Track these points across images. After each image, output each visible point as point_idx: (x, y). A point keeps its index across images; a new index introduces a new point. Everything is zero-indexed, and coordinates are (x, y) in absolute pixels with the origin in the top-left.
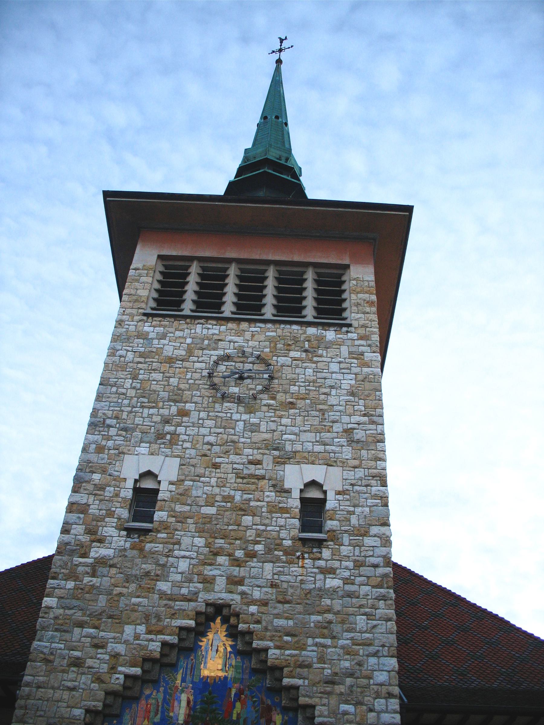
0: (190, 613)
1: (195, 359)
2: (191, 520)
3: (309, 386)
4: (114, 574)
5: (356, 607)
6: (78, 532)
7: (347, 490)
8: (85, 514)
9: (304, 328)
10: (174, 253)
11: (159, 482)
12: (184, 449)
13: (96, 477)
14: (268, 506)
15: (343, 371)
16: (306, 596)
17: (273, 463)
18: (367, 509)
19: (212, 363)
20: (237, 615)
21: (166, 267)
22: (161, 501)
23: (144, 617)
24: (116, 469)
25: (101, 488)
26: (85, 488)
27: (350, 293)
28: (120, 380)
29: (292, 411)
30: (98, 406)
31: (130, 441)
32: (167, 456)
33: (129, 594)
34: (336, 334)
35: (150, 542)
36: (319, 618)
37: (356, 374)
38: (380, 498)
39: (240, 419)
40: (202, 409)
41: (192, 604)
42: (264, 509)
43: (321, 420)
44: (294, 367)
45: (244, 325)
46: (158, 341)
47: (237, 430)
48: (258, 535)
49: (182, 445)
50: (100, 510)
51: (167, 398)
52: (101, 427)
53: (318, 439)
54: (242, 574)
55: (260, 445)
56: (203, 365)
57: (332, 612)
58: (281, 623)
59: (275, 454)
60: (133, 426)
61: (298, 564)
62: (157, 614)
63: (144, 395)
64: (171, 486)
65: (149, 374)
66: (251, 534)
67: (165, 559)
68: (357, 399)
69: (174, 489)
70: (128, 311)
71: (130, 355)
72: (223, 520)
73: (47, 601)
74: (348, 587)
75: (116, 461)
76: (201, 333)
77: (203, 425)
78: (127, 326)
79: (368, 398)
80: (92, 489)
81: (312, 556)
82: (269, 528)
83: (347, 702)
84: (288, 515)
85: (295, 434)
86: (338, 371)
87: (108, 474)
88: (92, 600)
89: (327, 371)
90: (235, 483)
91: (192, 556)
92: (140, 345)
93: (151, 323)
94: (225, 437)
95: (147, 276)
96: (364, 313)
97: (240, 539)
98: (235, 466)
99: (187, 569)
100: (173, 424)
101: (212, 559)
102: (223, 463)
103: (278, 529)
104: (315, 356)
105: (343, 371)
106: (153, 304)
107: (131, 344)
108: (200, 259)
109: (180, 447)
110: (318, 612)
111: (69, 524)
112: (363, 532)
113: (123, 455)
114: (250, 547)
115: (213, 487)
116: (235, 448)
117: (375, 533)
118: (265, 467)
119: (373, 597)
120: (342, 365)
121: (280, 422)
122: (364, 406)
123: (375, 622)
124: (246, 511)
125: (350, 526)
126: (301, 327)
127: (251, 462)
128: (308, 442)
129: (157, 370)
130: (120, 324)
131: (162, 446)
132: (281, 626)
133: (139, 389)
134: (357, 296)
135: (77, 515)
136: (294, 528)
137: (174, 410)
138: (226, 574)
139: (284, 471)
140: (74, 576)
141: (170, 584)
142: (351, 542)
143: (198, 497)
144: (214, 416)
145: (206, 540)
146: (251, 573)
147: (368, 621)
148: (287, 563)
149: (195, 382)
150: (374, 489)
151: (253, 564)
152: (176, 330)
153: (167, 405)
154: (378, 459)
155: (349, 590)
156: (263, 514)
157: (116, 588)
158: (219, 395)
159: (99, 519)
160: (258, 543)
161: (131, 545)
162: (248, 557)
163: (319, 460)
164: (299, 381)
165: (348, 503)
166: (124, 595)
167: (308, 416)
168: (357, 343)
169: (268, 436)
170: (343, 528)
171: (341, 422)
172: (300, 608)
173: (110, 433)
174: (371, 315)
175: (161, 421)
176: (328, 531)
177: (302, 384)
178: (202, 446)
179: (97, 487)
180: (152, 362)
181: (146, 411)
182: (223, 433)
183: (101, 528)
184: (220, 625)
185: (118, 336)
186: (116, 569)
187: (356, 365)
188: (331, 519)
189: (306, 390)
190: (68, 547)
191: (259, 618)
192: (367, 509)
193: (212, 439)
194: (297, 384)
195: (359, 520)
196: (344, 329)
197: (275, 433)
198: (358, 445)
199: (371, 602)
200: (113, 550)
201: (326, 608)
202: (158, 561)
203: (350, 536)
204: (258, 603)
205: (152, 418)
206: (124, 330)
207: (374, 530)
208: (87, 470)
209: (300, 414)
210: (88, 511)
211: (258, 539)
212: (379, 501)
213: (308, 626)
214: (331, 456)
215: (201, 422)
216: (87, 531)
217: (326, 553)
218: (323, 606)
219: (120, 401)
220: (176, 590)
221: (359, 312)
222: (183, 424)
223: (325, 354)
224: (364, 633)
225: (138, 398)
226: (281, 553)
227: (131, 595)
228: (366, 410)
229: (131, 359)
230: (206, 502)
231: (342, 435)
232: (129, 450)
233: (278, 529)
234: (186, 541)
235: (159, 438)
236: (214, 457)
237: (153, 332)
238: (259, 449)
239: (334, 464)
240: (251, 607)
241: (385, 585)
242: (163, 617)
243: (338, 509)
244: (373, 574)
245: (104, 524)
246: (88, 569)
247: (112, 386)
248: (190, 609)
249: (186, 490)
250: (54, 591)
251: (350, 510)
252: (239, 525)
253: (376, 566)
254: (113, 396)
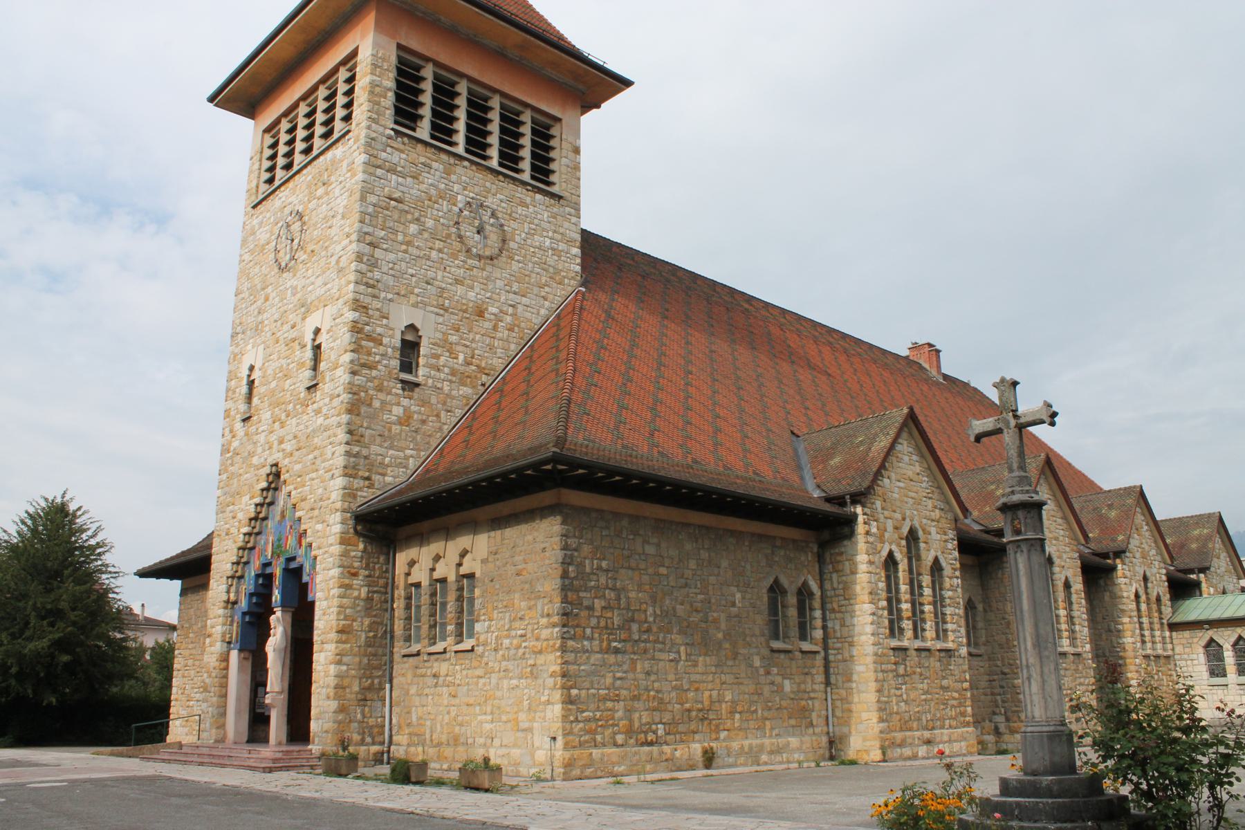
74: (328, 421)
83: (318, 522)
106: (264, 188)
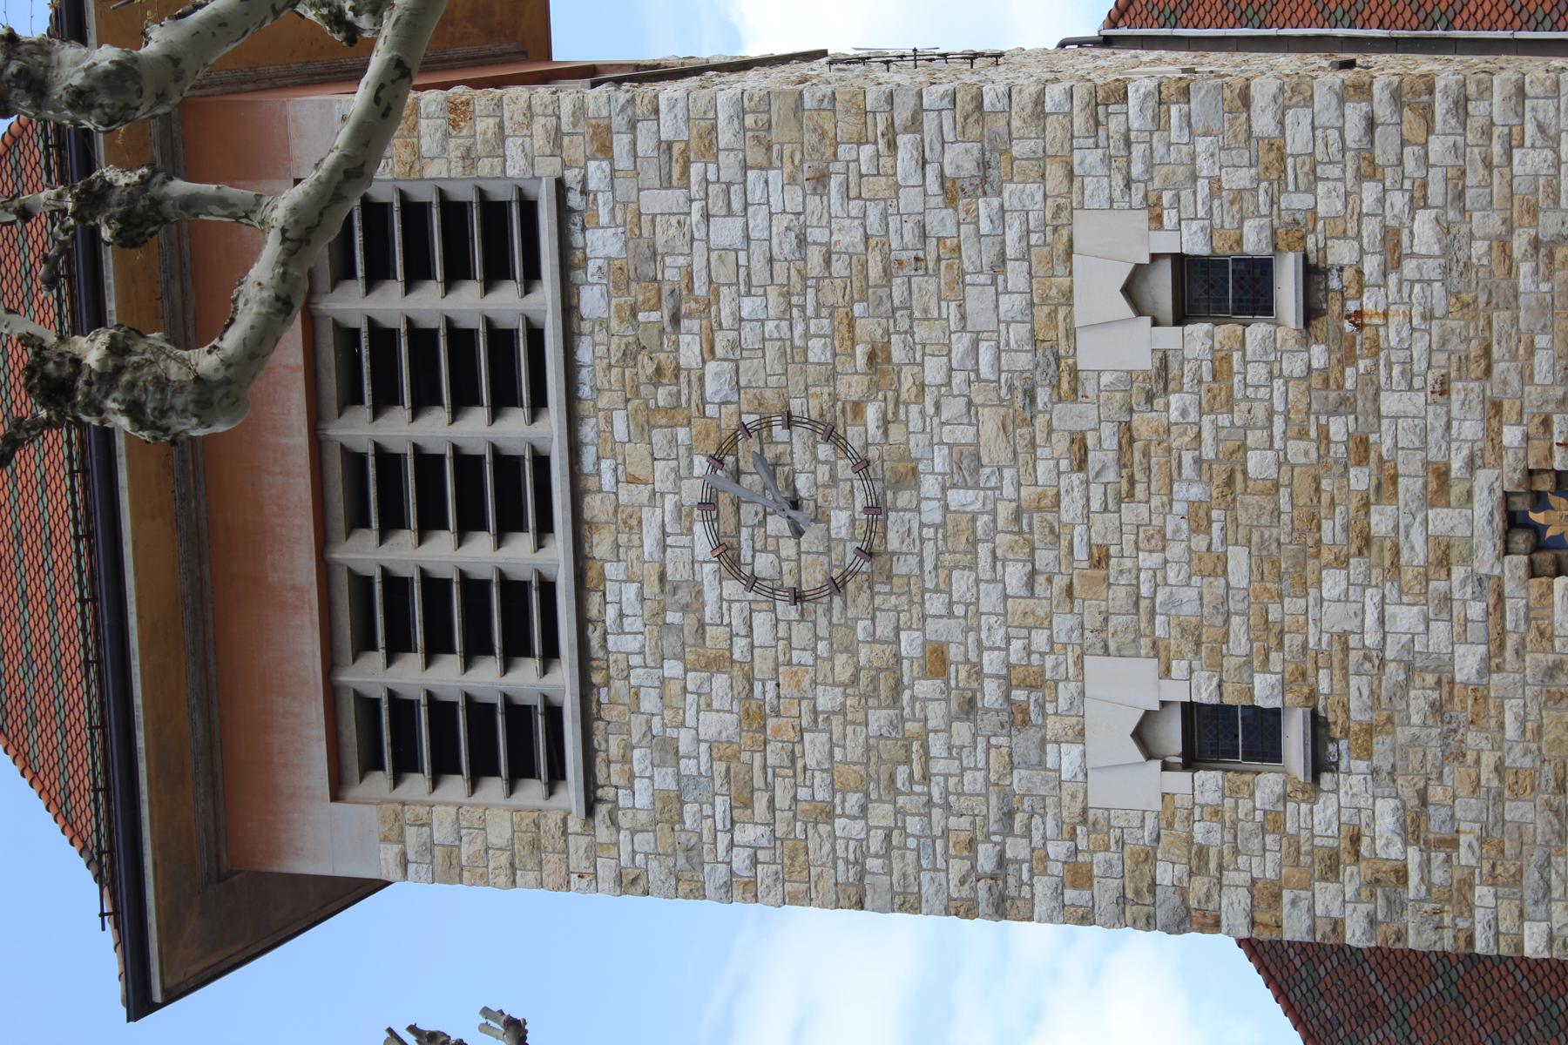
0: (1534, 593)
1: (740, 644)
2: (1270, 610)
3: (803, 308)
4: (1445, 790)
5: (1491, 174)
6: (1334, 899)
7: (1146, 197)
8: (1281, 888)
9: (586, 326)
10: (318, 752)
11: (1163, 704)
12: (1052, 649)
13: (1165, 874)
14: (1212, 411)
15: (737, 205)
16: (1468, 304)
17: (1075, 401)
18: (1202, 144)
19: (751, 596)
20: (1531, 474)
21: (372, 763)
22: (1221, 695)
23: (1556, 703)
24: (1136, 823)
25: (1199, 858)
26: (1203, 900)
27: (422, 179)
28: (840, 852)
29: (898, 354)
30: (938, 904)
31: (1044, 798)
32: (1082, 693)
33: (1496, 746)
34: (598, 226)
35: (1346, 709)
36: (1525, 268)
37: (745, 167)
38: (1164, 108)
39: (939, 500)
40: (916, 610)
41: (1509, 588)
42: (1224, 420)
43: (921, 272)
44: (738, 352)
45: (594, 507)
46: (683, 762)
47: (978, 506)
48: (1302, 434)
49: (1042, 654)
50: (1264, 850)
51: (891, 712)
52: (1005, 882)
53: (983, 279)
54: (1416, 467)
55: (1021, 443)
56: (761, 621)
57: (1508, 238)
58: (1545, 367)
59: (1046, 399)
60: (993, 801)
61: (1377, 326)
62: (1545, 674)
63: (884, 777)
64: (1174, 674)
65: (809, 774)
66: (1298, 451)
67: (1391, 668)
68: (836, 167)
69: (1184, 664)
70: (578, 860)
71: (748, 834)
72: (1266, 527)
73: (1534, 944)
74: (1436, 192)
75: (1110, 827)
76: (640, 637)
77: (971, 604)
78: (639, 858)
79: (831, 135)
80: (1206, 880)
81: (1352, 291)
82: (1279, 406)
84: (1236, 356)
85: (975, 344)
86: (739, 221)
87: (1155, 844)
88: (1521, 836)
89: (742, 255)
90: (1148, 502)
91: (1377, 599)
92: (707, 810)
93: (617, 787)
94: (1003, 540)
95: (430, 825)
96: (501, 134)
97: (1317, 481)
98: (1096, 505)
99: (1416, 609)
100: (975, 685)
101: (1381, 549)
102: (1089, 539)
103: (1278, 383)
104: (691, 290)
105: (737, 205)
106: (532, 791)
107: (706, 837)
108: (330, 664)
109: (1050, 661)
110: (1510, 273)
111: (1314, 923)
112: (1272, 155)
113: (1091, 814)
114: (1338, 451)
115: (1166, 561)
116: (1039, 509)
117: (1273, 123)
118: (1092, 425)
119: (1461, 131)
120: (717, 207)
121: (939, 386)
122: (859, 144)
123: (1530, 128)
124: (1232, 471)
125: (1256, 190)
126: (580, 334)
127: (1082, 464)
128: (997, 307)
129: (793, 751)
130: (634, 881)
131: (1050, 708)
132: (1554, 365)
133: (867, 795)
134: (432, 159)
135: (1286, 909)
136: (1275, 340)
137: (925, 687)
138: (1419, 509)
139: (1099, 372)
140: (1459, 890)
141: (1460, 650)
142: (1302, 187)
143: (1201, 599)
144: (937, 576)
145: (1328, 566)
146: (1411, 446)
147: (1528, 143)
148: (1377, 354)
149: (822, 639)
150: (1135, 124)
151: (1387, 443)
152: (636, 710)
153: (913, 709)
154: (1039, 108)
155: (1442, 191)
156: (1238, 422)
157: (1483, 782)
158: (866, 567)
159: (1292, 849)
160: (1324, 435)
161: (1358, 758)
162: (1367, 458)
163: (1053, 276)
164: (788, 335)
165: (1186, 194)
166: (1501, 760)
167: (910, 308)
168: (623, 162)
169: (989, 420)
170: (1264, 210)
171: (923, 213)
172: (1501, 318)
173: (1024, 853)
174: (507, 115)
175: (968, 720)
176: (1275, 247)
177: (799, 329)
178: (1039, 598)
179: (1198, 868)
180: (765, 767)
181: (938, 767)
182: (990, 545)
183: (1317, 841)
184: (1550, 512)
185: (678, 880)
186: (1430, 789)
187: (712, 168)
188: (1239, 242)
189: (818, 316)
190: (1380, 917)
191: (1537, 420)
192: (1202, 144)
193: (1014, 575)
194: (798, 342)
195: (1234, 166)
196: (574, 200)
197: (978, 400)
198: (993, 164)
199: (1474, 137)
200: (1379, 802)
201: (1495, 253)
202: (1397, 684)
203: (1287, 191)
204: (1495, 423)
205: (963, 747)
206: (653, 864)
207: (1263, 123)
208: (1148, 900)
209: (906, 332)
210: (1272, 881)
211: (1313, 433)
212: (1174, 110)
213: (1548, 298)
214: (1040, 242)
215: (959, 610)
216: (1329, 875)
217: (1341, 253)
218: (1490, 262)
219: (912, 843)
220: (1476, 631)
221: (500, 152)
222: (973, 658)
223: (681, 261)
224: (1559, 158)
225: (899, 793)
226: (1349, 371)
227: (1498, 744)
228: (871, 139)
229: (760, 830)
230: (1213, 574)
231: (967, 212)
232: (1074, 797)
233: (1278, 383)
234: (1335, 617)
235: (1026, 722)
236: (1071, 564)
237: (651, 778)
238: (1033, 444)
239: (1065, 232)
240: (1506, 442)
241: (1425, 98)
242: (1551, 657)
243: (1207, 222)
244: (1394, 131)
245: (1304, 835)
246: (1438, 858)
247: (862, 874)
248: (1523, 593)
249: (1183, 630)
250: (1505, 934)
251: (1207, 190)
252: (1277, 486)
253: (1371, 124)
254: (897, 866)
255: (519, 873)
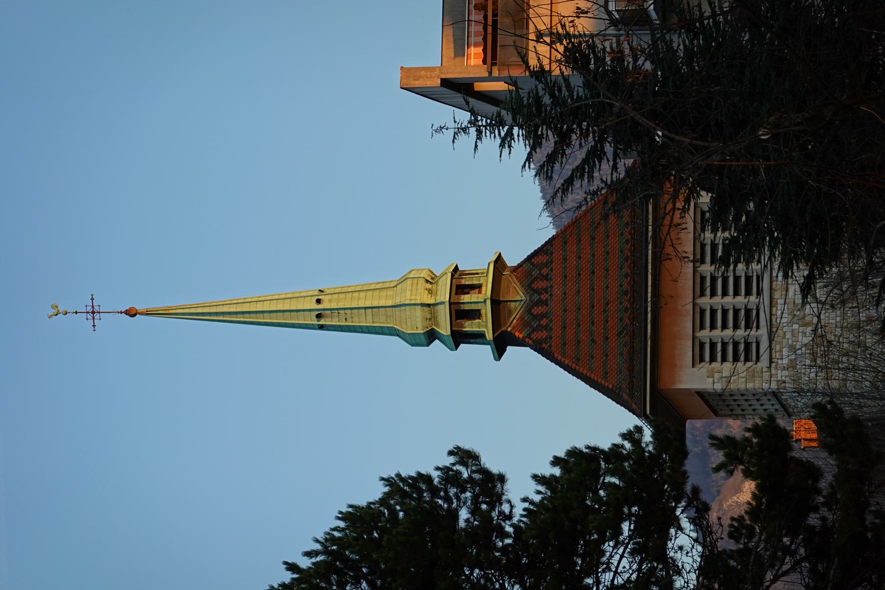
10: (690, 354)
255: (748, 384)
